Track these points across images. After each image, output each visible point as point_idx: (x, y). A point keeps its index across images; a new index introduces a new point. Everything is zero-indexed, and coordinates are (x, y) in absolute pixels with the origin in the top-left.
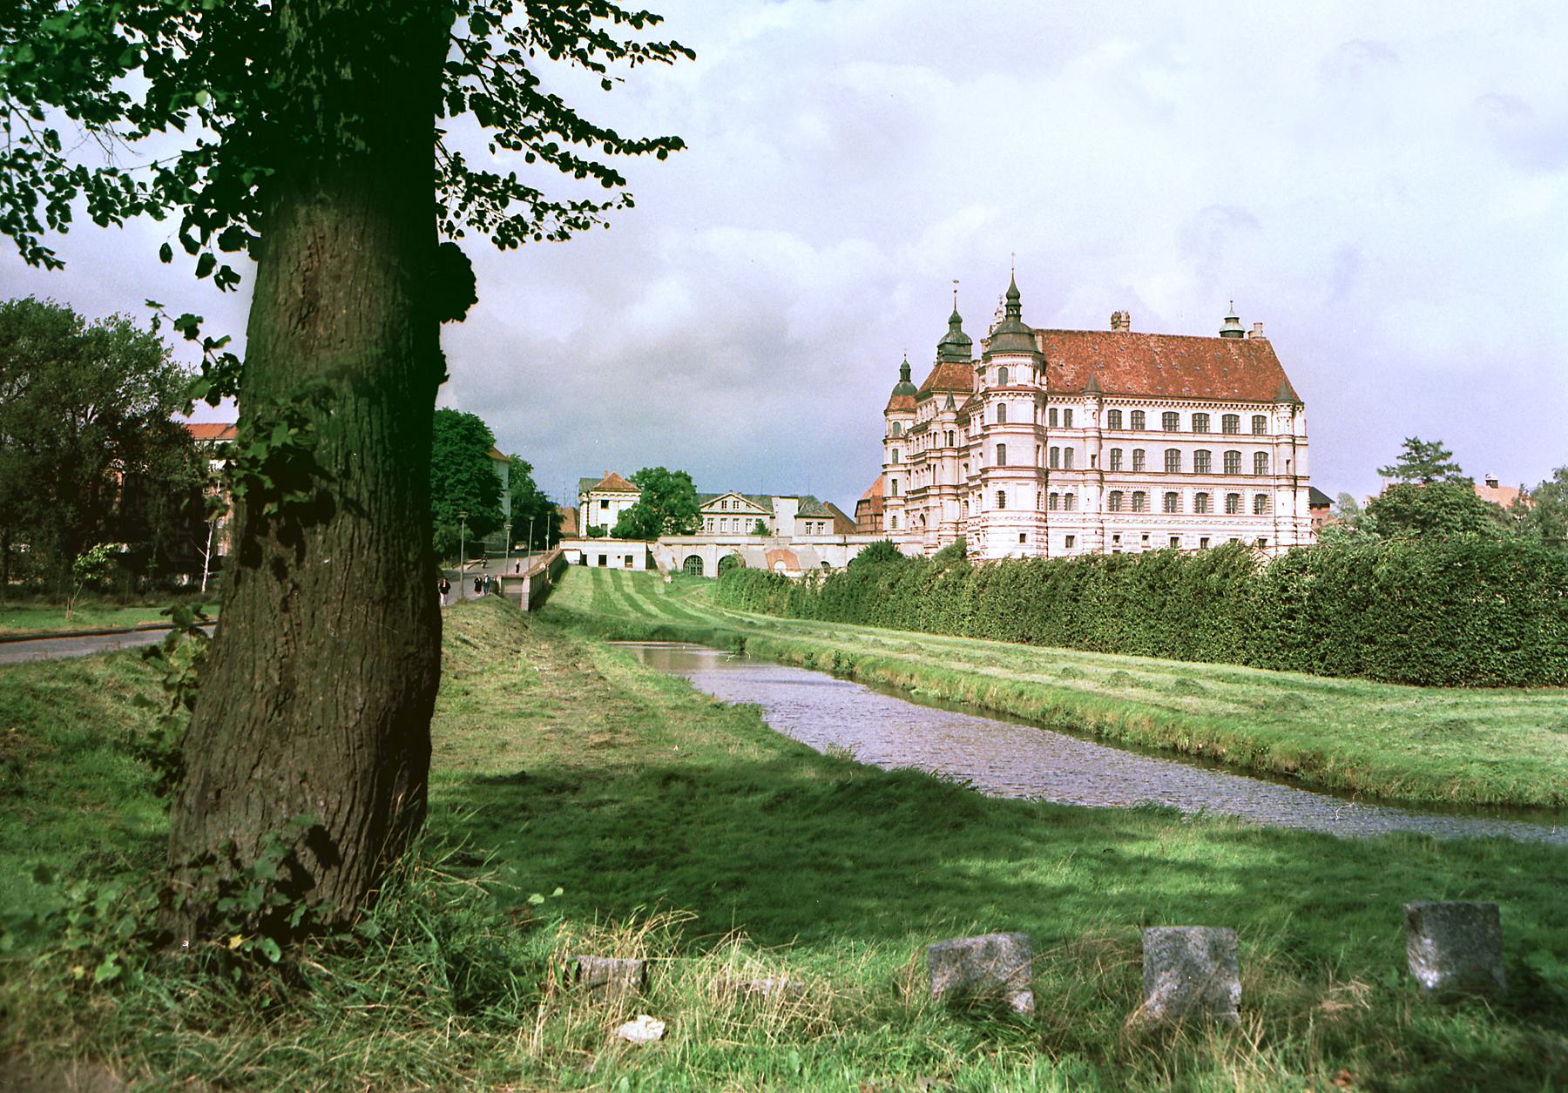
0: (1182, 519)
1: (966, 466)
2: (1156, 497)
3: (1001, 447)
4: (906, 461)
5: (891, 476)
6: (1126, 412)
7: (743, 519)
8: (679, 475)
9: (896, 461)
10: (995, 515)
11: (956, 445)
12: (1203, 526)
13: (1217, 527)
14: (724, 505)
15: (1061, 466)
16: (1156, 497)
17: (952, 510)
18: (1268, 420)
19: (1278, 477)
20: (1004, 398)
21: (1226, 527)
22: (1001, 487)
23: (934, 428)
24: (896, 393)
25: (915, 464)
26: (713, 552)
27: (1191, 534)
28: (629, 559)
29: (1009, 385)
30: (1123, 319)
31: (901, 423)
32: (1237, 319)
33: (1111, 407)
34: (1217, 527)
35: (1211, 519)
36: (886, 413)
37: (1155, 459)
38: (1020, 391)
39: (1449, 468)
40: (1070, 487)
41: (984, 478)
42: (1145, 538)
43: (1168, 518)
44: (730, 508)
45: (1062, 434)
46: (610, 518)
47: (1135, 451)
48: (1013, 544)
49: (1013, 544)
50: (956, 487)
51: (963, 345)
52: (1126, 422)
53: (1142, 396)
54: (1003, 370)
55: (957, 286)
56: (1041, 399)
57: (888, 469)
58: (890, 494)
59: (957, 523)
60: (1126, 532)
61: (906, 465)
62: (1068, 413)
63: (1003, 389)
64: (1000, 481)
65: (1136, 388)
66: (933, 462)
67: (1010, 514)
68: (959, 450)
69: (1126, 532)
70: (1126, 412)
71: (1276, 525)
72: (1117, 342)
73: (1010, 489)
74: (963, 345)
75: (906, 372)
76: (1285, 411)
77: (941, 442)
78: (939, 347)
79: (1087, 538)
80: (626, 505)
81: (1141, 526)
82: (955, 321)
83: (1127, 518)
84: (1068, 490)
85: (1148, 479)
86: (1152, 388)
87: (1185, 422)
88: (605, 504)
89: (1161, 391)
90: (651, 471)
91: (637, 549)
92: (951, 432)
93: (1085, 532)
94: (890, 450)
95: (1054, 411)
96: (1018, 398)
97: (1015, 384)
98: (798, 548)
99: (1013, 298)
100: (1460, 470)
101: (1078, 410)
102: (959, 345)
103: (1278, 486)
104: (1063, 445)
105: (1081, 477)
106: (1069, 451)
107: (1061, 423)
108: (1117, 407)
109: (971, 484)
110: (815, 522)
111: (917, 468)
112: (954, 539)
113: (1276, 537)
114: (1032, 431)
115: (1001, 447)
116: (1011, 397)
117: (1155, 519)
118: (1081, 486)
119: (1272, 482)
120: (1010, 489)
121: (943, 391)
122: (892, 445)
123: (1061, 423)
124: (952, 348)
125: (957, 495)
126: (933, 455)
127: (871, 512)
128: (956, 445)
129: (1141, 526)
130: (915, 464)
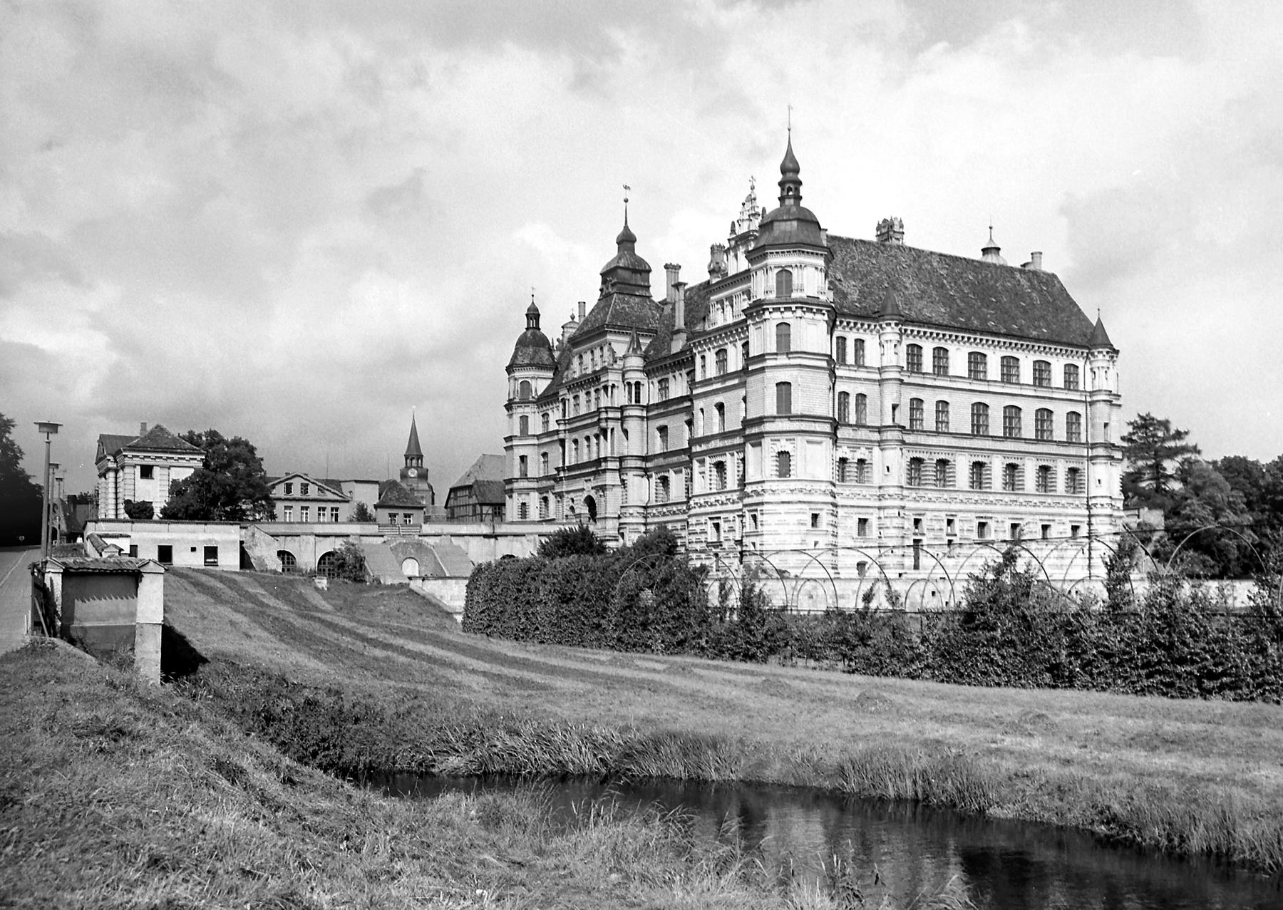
0: (991, 498)
1: (663, 430)
3: (784, 387)
4: (556, 427)
5: (518, 452)
6: (928, 347)
7: (314, 507)
8: (237, 443)
10: (774, 486)
11: (644, 402)
13: (998, 508)
14: (288, 489)
15: (852, 419)
17: (641, 489)
18: (1081, 371)
19: (1093, 446)
21: (1008, 508)
22: (784, 445)
23: (613, 378)
24: (522, 343)
26: (311, 547)
27: (1000, 517)
28: (211, 552)
29: (795, 295)
30: (896, 228)
31: (533, 383)
32: (998, 249)
33: (911, 341)
34: (998, 508)
35: (1021, 499)
36: (510, 369)
37: (960, 419)
38: (809, 305)
39: (1184, 449)
40: (863, 449)
41: (751, 431)
42: (950, 522)
43: (976, 497)
44: (296, 492)
45: (853, 374)
46: (156, 492)
47: (938, 402)
48: (804, 528)
49: (804, 528)
50: (645, 459)
51: (640, 272)
52: (927, 363)
54: (785, 274)
55: (628, 194)
56: (836, 316)
57: (515, 442)
58: (517, 475)
59: (645, 508)
60: (929, 515)
61: (557, 432)
62: (860, 343)
63: (786, 299)
64: (783, 438)
65: (936, 318)
67: (799, 485)
68: (648, 408)
69: (960, 515)
70: (928, 347)
71: (1089, 508)
73: (799, 449)
74: (640, 272)
75: (533, 315)
76: (1101, 359)
77: (621, 397)
78: (605, 275)
79: (887, 522)
80: (183, 474)
81: (945, 506)
82: (626, 240)
83: (930, 495)
84: (862, 453)
86: (953, 318)
87: (994, 368)
88: (147, 472)
89: (965, 323)
90: (200, 436)
91: (226, 536)
92: (638, 384)
93: (882, 514)
94: (516, 418)
95: (842, 340)
97: (804, 295)
98: (431, 541)
100: (1199, 452)
101: (871, 341)
102: (635, 271)
103: (1091, 459)
104: (853, 389)
105: (876, 436)
106: (861, 397)
107: (850, 359)
108: (917, 341)
109: (696, 449)
110: (401, 512)
111: (575, 436)
112: (643, 529)
113: (1090, 524)
114: (824, 364)
115: (784, 387)
116: (799, 313)
117: (961, 496)
118: (876, 449)
120: (799, 449)
121: (620, 330)
122: (519, 412)
123: (850, 359)
124: (626, 274)
125: (646, 470)
126: (611, 415)
127: (474, 500)
128: (644, 402)
129: (945, 506)
130: (571, 431)
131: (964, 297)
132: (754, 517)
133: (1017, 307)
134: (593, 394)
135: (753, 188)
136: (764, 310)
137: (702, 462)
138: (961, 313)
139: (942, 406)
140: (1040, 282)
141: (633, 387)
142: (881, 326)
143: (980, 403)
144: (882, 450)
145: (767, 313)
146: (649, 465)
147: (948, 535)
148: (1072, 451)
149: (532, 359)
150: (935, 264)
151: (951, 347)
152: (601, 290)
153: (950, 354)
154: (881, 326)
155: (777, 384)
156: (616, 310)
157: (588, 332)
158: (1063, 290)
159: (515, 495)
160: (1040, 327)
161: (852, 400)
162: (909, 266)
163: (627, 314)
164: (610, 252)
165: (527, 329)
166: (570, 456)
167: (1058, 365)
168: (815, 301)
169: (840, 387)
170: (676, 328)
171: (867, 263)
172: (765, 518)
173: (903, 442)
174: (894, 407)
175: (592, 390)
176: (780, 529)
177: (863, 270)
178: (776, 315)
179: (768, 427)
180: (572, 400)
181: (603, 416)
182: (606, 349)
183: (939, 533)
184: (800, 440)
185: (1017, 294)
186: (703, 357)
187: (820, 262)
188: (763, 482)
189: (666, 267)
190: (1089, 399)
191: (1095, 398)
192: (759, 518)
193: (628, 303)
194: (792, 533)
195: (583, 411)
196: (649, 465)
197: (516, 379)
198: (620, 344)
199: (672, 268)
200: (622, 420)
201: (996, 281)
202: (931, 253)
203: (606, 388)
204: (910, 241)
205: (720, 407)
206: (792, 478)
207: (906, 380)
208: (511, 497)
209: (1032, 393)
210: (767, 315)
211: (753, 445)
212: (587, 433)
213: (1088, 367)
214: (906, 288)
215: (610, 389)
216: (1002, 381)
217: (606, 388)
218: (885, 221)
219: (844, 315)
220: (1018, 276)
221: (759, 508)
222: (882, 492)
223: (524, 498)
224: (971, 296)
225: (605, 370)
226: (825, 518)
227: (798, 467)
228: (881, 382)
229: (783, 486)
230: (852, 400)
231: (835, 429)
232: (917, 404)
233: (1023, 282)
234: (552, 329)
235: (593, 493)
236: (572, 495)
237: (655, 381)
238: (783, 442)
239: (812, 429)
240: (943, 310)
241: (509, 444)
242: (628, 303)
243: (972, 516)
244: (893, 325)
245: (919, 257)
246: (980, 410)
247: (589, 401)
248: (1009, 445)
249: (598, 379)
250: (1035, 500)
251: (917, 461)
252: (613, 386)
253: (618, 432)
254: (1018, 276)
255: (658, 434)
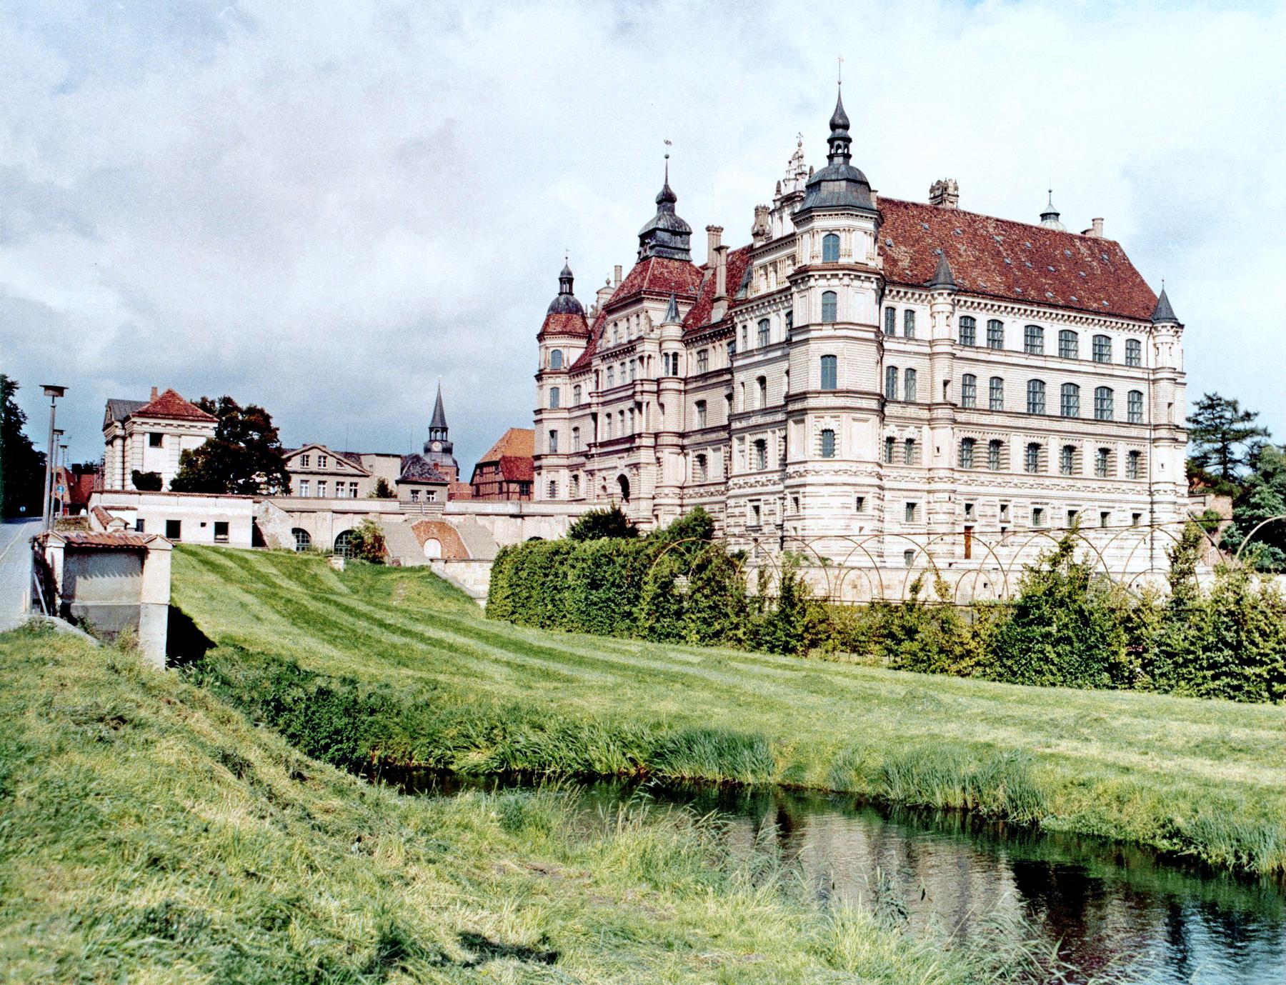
0: (1047, 482)
1: (701, 404)
2: (1016, 447)
3: (829, 359)
5: (548, 426)
6: (982, 319)
7: (332, 481)
8: (252, 411)
9: (555, 406)
10: (817, 466)
11: (681, 374)
12: (1071, 493)
13: (1054, 493)
14: (305, 461)
15: (901, 395)
17: (678, 468)
18: (1143, 346)
19: (1156, 427)
20: (835, 282)
22: (828, 423)
23: (648, 348)
24: (554, 309)
25: (604, 404)
27: (1056, 503)
28: (222, 528)
29: (842, 261)
30: (951, 191)
31: (565, 352)
34: (1054, 493)
35: (1079, 484)
36: (541, 337)
37: (1016, 397)
38: (857, 271)
39: (1253, 432)
40: (912, 428)
42: (1003, 508)
43: (1031, 481)
44: (313, 466)
45: (902, 347)
46: (166, 464)
49: (847, 512)
50: (682, 435)
52: (981, 337)
54: (832, 237)
56: (885, 283)
57: (545, 415)
58: (546, 450)
59: (681, 488)
61: (589, 405)
62: (910, 314)
63: (833, 268)
64: (827, 415)
65: (989, 286)
66: (646, 398)
67: (844, 466)
68: (686, 381)
69: (1014, 500)
71: (1151, 494)
72: (949, 221)
73: (844, 427)
74: (680, 234)
76: (1165, 333)
77: (657, 368)
78: (644, 237)
79: (937, 507)
82: (667, 200)
83: (983, 478)
84: (910, 432)
86: (1009, 288)
87: (1051, 343)
91: (237, 510)
92: (675, 355)
93: (932, 497)
94: (547, 389)
96: (857, 283)
98: (454, 520)
100: (1269, 435)
101: (922, 312)
102: (674, 233)
103: (1155, 440)
104: (902, 363)
105: (925, 414)
107: (900, 330)
108: (970, 313)
109: (736, 425)
110: (424, 489)
111: (608, 409)
113: (1152, 512)
114: (872, 336)
115: (829, 359)
116: (846, 280)
117: (1016, 480)
118: (926, 428)
119: (1146, 434)
120: (844, 427)
122: (549, 382)
124: (664, 236)
125: (683, 448)
126: (646, 387)
127: (500, 477)
128: (681, 374)
130: (604, 404)
131: (1021, 267)
132: (796, 500)
133: (1077, 277)
134: (628, 364)
135: (800, 145)
136: (809, 277)
137: (742, 439)
138: (1016, 281)
139: (997, 382)
140: (1101, 251)
141: (671, 358)
142: (932, 295)
143: (1037, 380)
144: (932, 429)
145: (812, 280)
146: (686, 442)
147: (1001, 522)
148: (1133, 432)
149: (565, 327)
150: (991, 230)
151: (1007, 319)
152: (639, 253)
153: (1005, 327)
154: (932, 295)
155: (822, 357)
156: (653, 275)
157: (624, 298)
158: (1124, 257)
159: (544, 472)
160: (1101, 300)
161: (901, 375)
162: (964, 231)
163: (666, 280)
164: (648, 214)
165: (561, 294)
166: (602, 429)
167: (1119, 338)
168: (863, 267)
169: (889, 360)
170: (717, 296)
171: (919, 227)
172: (808, 500)
173: (955, 421)
174: (946, 383)
175: (627, 360)
176: (823, 512)
177: (915, 235)
178: (823, 282)
179: (811, 402)
180: (606, 371)
181: (638, 388)
182: (642, 316)
183: (992, 520)
184: (844, 416)
185: (1076, 262)
186: (745, 327)
187: (870, 226)
188: (806, 462)
189: (708, 229)
190: (1152, 377)
191: (1158, 376)
192: (801, 501)
193: (667, 267)
194: (835, 517)
195: (617, 383)
196: (686, 442)
197: (547, 348)
198: (657, 311)
199: (714, 230)
200: (658, 392)
201: (1055, 249)
202: (987, 218)
203: (641, 358)
205: (762, 380)
206: (836, 458)
207: (959, 354)
208: (539, 474)
209: (1093, 370)
210: (812, 282)
211: (796, 422)
212: (621, 406)
213: (1151, 341)
214: (960, 255)
215: (646, 360)
216: (1060, 357)
217: (641, 358)
218: (939, 182)
219: (894, 283)
220: (1078, 243)
221: (801, 490)
222: (932, 474)
223: (553, 476)
224: (1028, 264)
225: (641, 338)
226: (870, 502)
227: (843, 447)
228: (931, 356)
229: (826, 466)
230: (901, 375)
231: (883, 406)
232: (969, 379)
233: (1083, 250)
234: (587, 296)
235: (626, 472)
236: (604, 473)
237: (694, 351)
238: (827, 419)
239: (858, 405)
240: (998, 279)
241: (539, 417)
242: (667, 267)
243: (1027, 501)
244: (945, 295)
245: (975, 222)
246: (1036, 387)
247: (623, 372)
248: (1067, 425)
249: (633, 349)
250: (1094, 485)
251: (969, 442)
252: (649, 357)
253: (654, 406)
254: (1078, 243)
255: (696, 408)
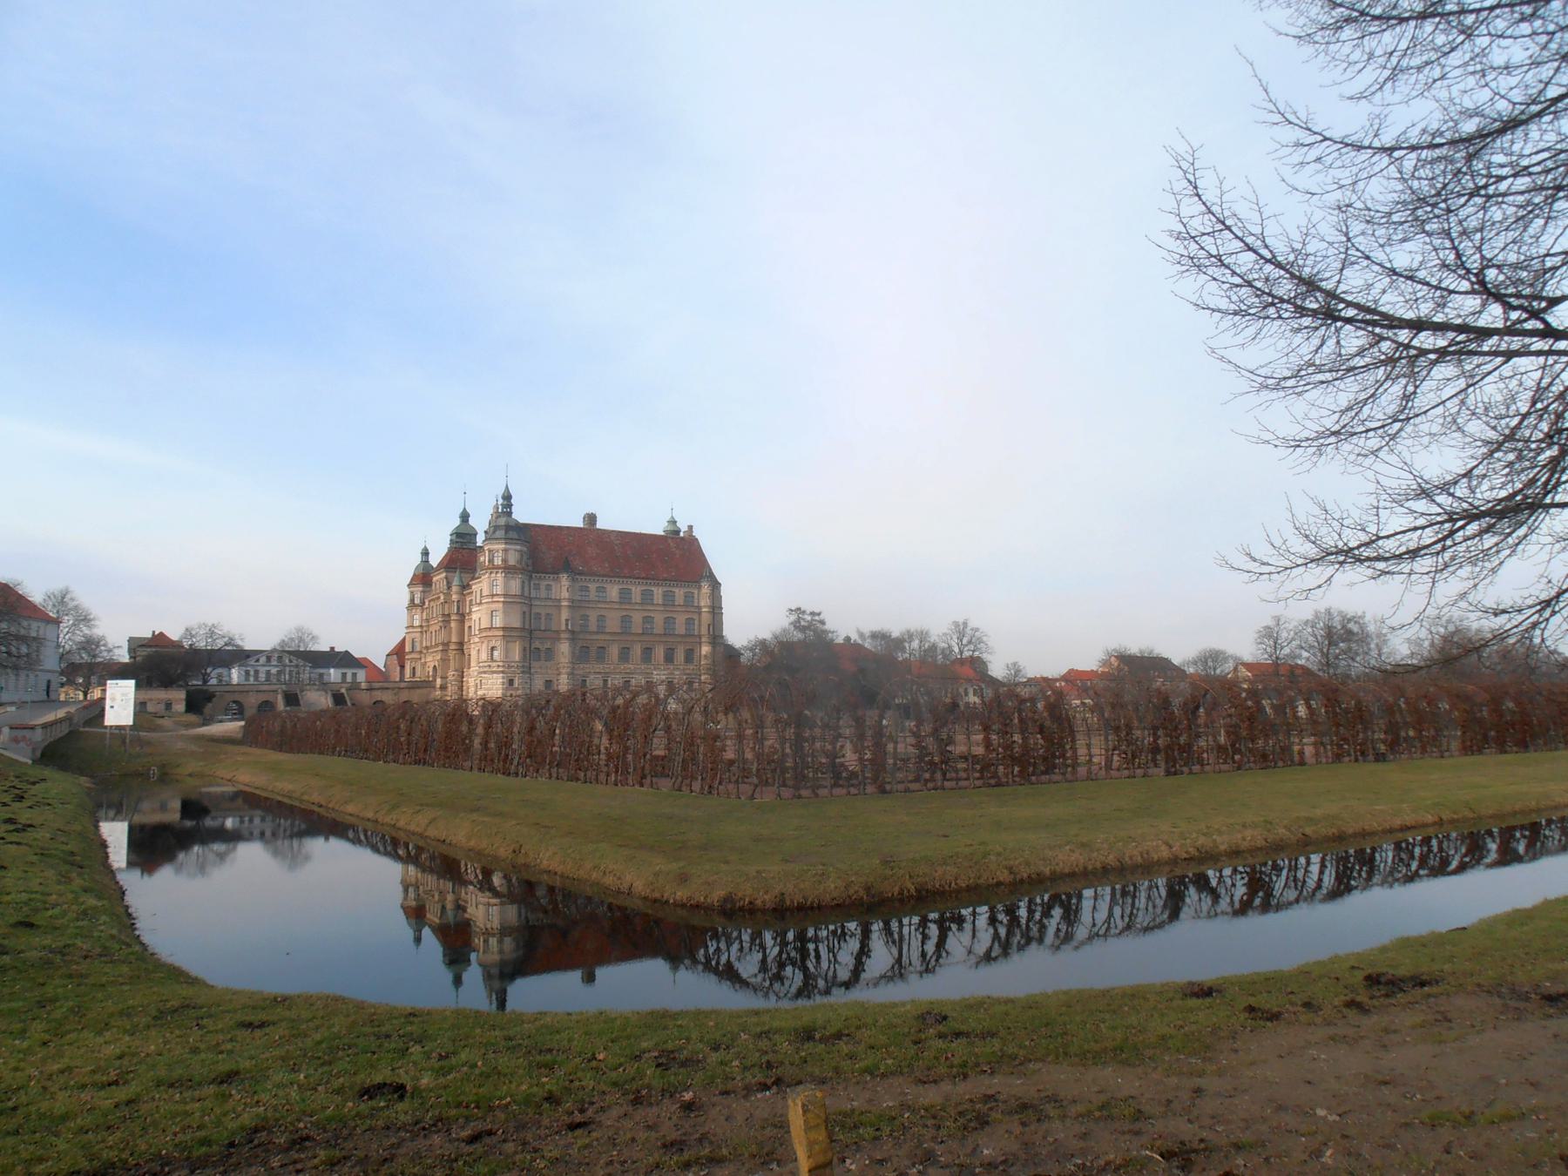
2: (614, 651)
16: (614, 651)
53: (604, 576)
75: (425, 553)
82: (465, 517)
84: (548, 645)
85: (608, 637)
99: (507, 497)
139: (601, 618)
151: (608, 586)
174: (567, 620)
204: (600, 525)
254: (670, 541)
